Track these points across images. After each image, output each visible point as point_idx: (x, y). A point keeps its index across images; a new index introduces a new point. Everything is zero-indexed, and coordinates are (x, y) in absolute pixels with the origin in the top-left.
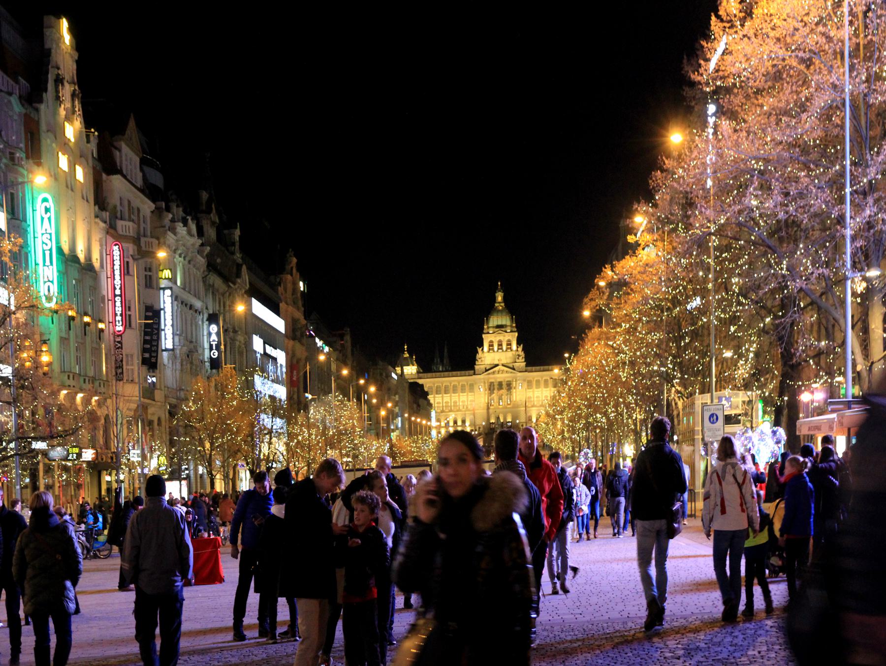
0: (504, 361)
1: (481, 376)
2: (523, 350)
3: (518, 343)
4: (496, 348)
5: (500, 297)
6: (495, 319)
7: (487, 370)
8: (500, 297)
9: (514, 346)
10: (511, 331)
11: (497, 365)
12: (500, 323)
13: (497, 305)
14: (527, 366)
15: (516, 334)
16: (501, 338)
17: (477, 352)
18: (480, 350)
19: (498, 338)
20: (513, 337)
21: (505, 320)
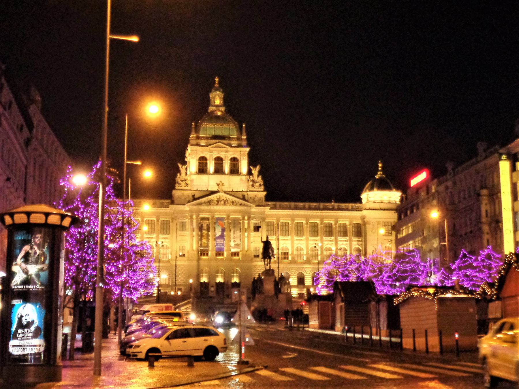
0: (226, 188)
1: (187, 208)
2: (260, 173)
3: (252, 162)
4: (211, 167)
5: (217, 99)
6: (210, 126)
7: (194, 199)
8: (217, 99)
9: (244, 166)
10: (239, 146)
11: (213, 193)
12: (218, 133)
13: (211, 109)
14: (268, 198)
15: (248, 149)
16: (222, 155)
17: (179, 171)
18: (182, 169)
19: (215, 155)
20: (243, 155)
21: (229, 129)
